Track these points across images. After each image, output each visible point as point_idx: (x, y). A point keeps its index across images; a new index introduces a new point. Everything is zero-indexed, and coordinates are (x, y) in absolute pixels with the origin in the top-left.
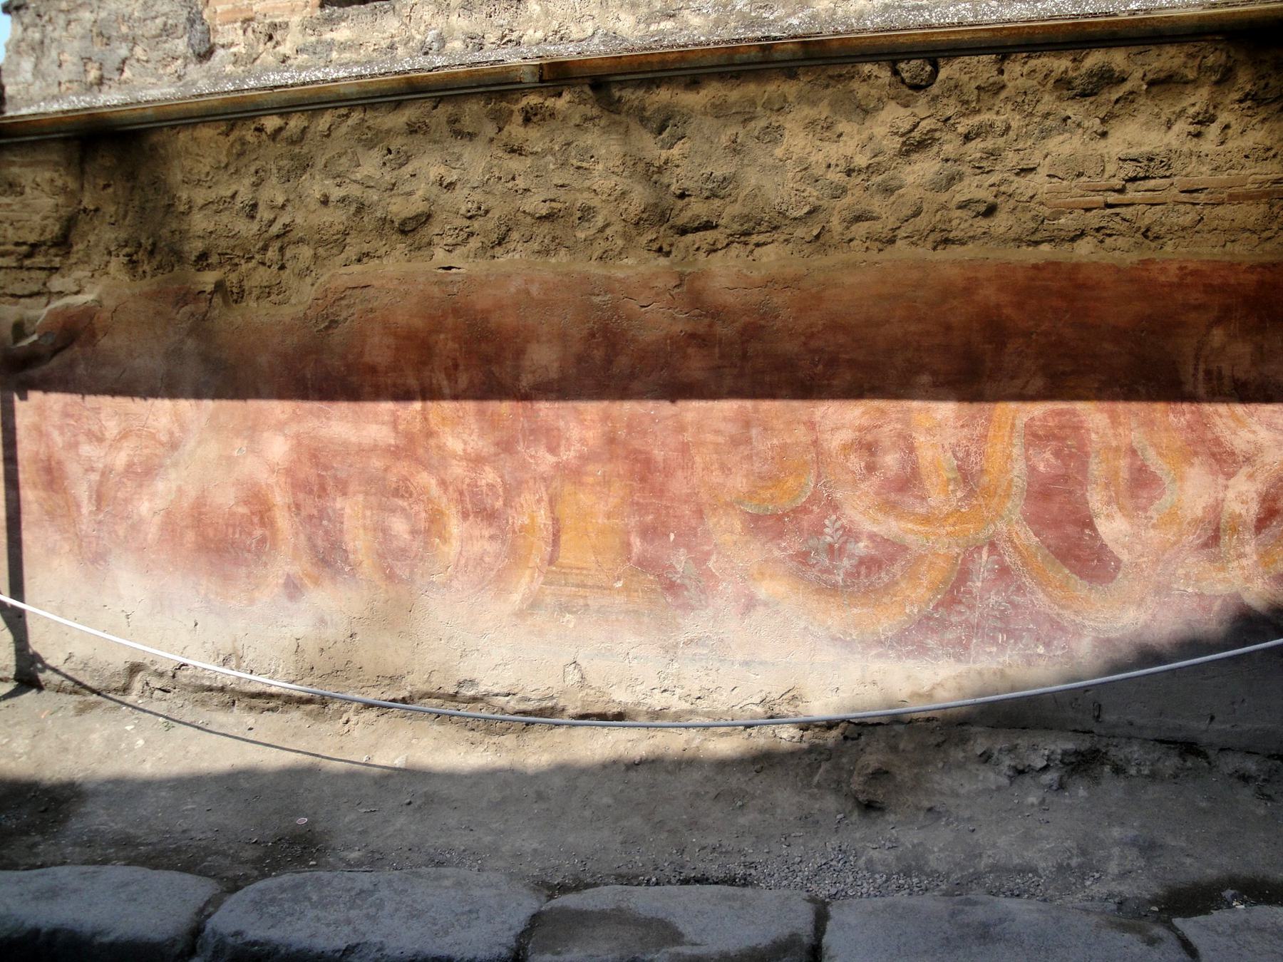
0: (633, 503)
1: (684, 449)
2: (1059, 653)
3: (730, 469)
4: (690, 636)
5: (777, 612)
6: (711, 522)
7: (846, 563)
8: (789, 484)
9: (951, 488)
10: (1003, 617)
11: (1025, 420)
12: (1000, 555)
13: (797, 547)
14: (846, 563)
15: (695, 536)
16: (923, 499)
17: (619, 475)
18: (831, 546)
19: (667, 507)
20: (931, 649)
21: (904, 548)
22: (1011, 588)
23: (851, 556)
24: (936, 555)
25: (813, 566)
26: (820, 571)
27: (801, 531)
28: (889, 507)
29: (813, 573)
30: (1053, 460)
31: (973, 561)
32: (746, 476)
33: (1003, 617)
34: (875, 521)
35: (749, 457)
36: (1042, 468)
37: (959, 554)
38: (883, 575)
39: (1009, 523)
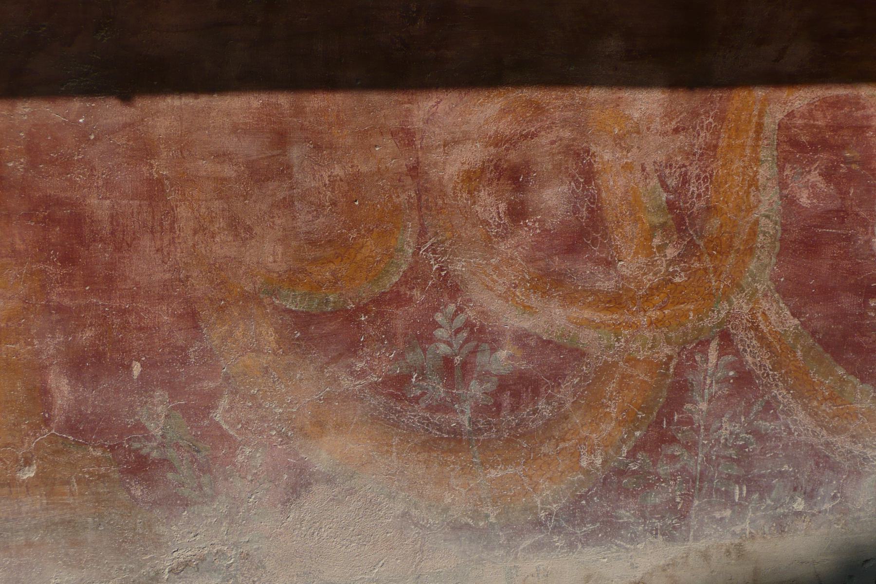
0: (47, 307)
1: (154, 192)
2: (827, 506)
3: (249, 229)
4: (184, 555)
5: (351, 492)
6: (214, 335)
7: (476, 389)
8: (365, 252)
9: (656, 241)
10: (742, 457)
11: (780, 116)
12: (737, 353)
13: (385, 367)
14: (476, 389)
15: (184, 362)
16: (609, 264)
17: (15, 253)
18: (447, 361)
19: (122, 312)
20: (626, 526)
21: (579, 354)
22: (755, 408)
23: (484, 377)
24: (632, 361)
25: (416, 399)
26: (429, 408)
27: (391, 337)
28: (549, 283)
29: (414, 415)
30: (822, 185)
31: (694, 367)
32: (283, 240)
33: (742, 457)
34: (527, 309)
35: (288, 204)
36: (804, 200)
37: (670, 358)
38: (541, 405)
39: (752, 297)
